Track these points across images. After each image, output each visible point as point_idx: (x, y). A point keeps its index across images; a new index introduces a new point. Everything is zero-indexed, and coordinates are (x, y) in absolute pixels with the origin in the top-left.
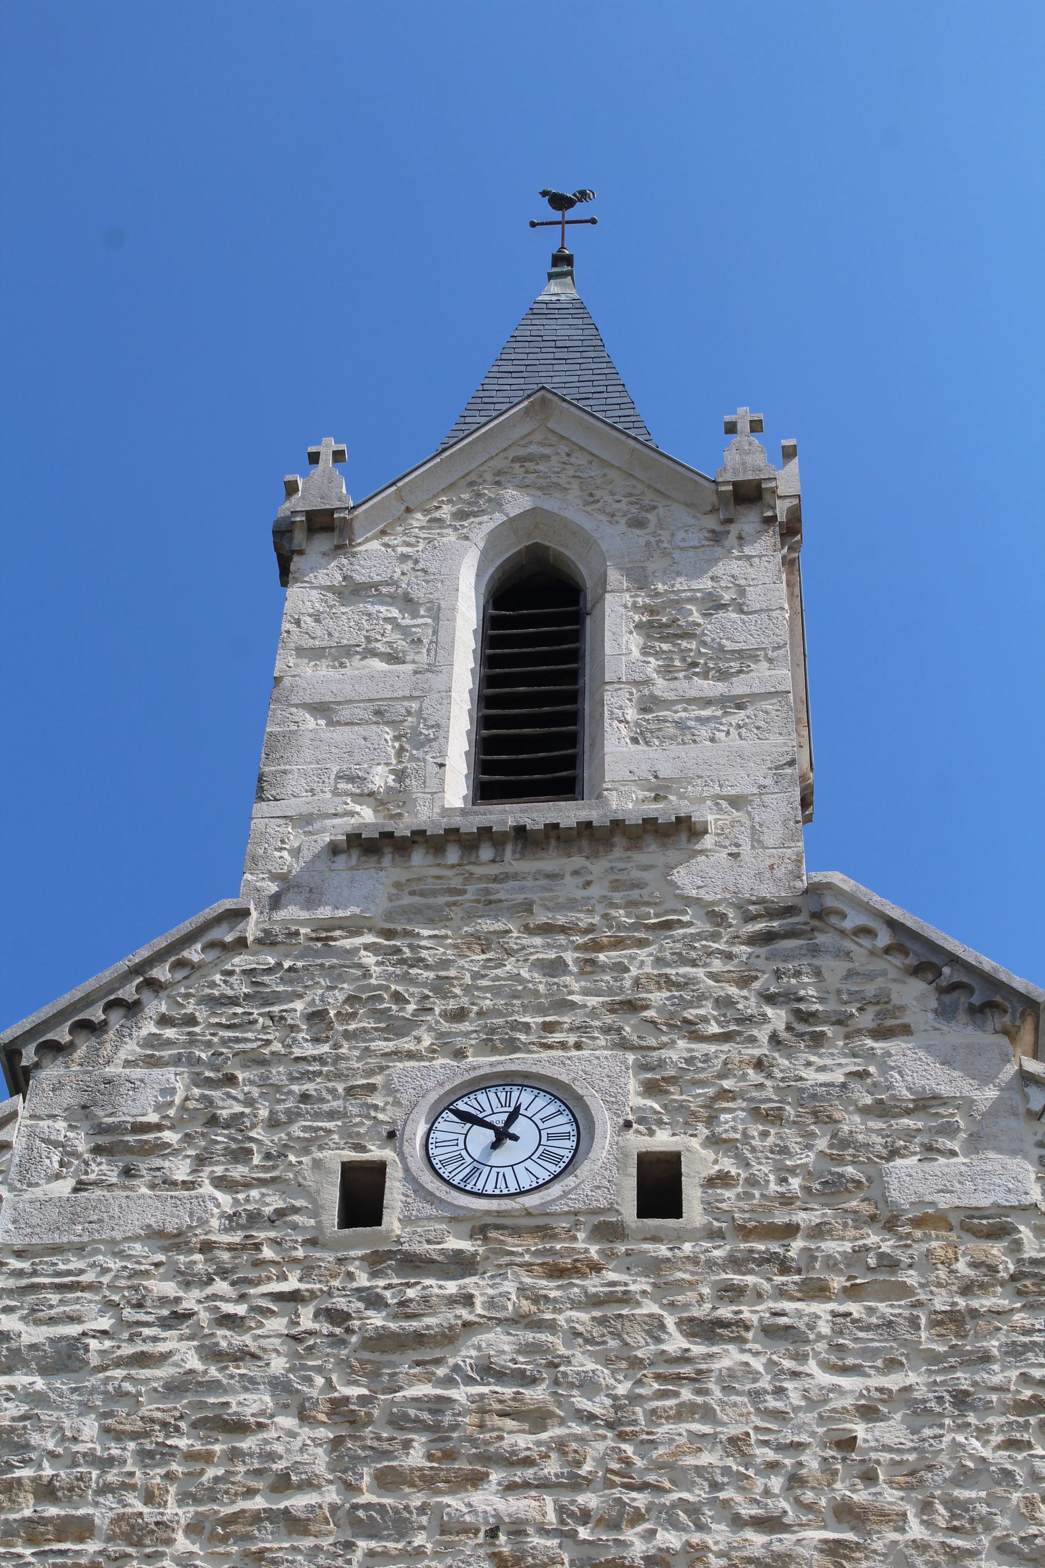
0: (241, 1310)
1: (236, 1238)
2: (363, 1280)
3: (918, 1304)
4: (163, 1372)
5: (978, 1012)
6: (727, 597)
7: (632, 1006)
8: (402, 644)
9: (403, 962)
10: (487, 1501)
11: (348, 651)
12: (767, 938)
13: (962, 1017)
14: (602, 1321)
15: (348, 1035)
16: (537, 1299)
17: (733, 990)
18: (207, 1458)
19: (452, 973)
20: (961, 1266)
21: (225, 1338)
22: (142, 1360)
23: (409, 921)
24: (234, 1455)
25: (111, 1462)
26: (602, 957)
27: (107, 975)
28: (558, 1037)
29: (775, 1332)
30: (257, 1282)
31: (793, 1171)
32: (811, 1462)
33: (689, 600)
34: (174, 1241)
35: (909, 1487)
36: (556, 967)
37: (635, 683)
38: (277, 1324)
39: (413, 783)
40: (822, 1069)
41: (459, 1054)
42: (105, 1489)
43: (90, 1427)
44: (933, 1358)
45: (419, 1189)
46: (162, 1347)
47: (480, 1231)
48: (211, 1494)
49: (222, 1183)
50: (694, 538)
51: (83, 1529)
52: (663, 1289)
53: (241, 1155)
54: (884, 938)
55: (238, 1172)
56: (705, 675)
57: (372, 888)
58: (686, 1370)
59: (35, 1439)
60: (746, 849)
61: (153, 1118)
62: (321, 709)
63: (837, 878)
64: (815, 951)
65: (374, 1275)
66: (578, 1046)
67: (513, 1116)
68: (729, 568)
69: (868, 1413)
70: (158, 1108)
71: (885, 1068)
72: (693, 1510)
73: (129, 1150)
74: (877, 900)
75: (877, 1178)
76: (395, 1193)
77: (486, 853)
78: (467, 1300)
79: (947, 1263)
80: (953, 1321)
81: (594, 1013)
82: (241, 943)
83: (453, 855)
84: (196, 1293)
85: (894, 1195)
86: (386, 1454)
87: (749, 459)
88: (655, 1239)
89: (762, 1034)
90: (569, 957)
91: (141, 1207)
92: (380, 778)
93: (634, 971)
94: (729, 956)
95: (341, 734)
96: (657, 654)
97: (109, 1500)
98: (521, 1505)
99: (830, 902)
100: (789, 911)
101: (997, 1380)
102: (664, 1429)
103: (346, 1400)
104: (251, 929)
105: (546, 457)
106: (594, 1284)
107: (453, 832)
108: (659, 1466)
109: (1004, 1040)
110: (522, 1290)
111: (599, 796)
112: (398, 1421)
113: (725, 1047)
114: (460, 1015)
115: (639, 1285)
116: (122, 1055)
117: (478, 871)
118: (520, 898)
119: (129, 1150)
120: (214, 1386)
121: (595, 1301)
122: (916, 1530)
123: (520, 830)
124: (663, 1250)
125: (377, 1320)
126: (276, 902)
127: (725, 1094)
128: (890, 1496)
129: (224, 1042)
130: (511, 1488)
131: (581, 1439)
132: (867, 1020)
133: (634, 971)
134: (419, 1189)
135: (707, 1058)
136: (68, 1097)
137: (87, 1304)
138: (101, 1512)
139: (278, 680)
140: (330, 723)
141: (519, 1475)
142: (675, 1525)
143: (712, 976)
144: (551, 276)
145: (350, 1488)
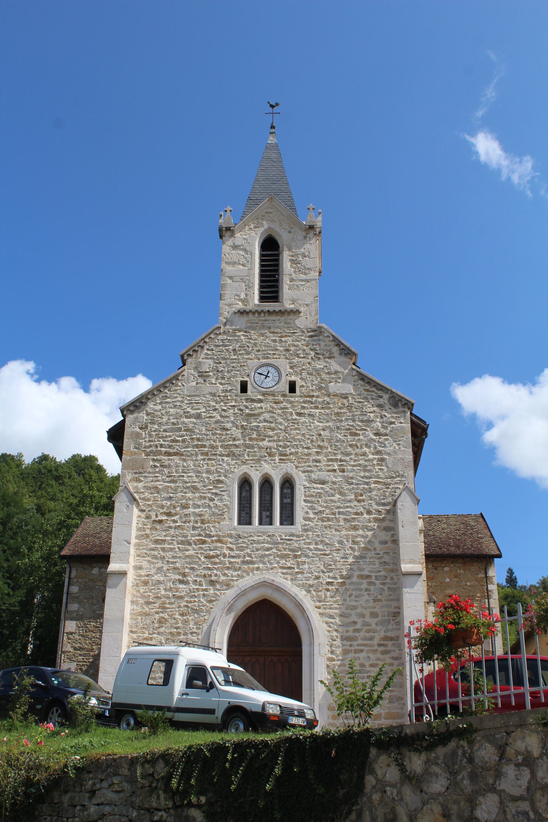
0: (225, 408)
1: (223, 394)
2: (245, 403)
3: (332, 411)
4: (214, 419)
5: (346, 355)
6: (307, 254)
7: (288, 350)
8: (245, 262)
9: (248, 338)
10: (265, 443)
11: (235, 263)
12: (311, 336)
13: (343, 355)
14: (283, 412)
15: (240, 354)
16: (273, 408)
17: (305, 348)
18: (222, 435)
19: (257, 342)
20: (339, 404)
21: (224, 413)
22: (211, 417)
23: (249, 329)
24: (227, 434)
25: (207, 435)
26: (283, 339)
27: (198, 340)
28: (275, 356)
29: (310, 415)
30: (228, 403)
31: (314, 385)
32: (314, 438)
33: (300, 254)
34: (214, 395)
35: (329, 443)
36: (275, 341)
37: (289, 275)
38: (231, 411)
39: (248, 297)
40: (320, 365)
41: (259, 359)
42: (207, 440)
43: (204, 429)
44: (335, 420)
45: (253, 386)
46: (214, 415)
47: (263, 395)
48: (224, 441)
49: (220, 384)
50: (301, 238)
51: (205, 446)
52: (293, 407)
53: (223, 378)
54: (331, 338)
55: (223, 381)
56: (302, 274)
57: (242, 321)
58: (296, 422)
59: (195, 431)
60: (308, 317)
61: (208, 370)
62: (231, 278)
63: (324, 325)
64: (319, 340)
65: (247, 402)
66: (279, 358)
67: (269, 372)
68: (307, 246)
69: (324, 430)
70: (209, 368)
71: (330, 365)
72: (297, 445)
73: (205, 376)
74: (331, 330)
75: (327, 386)
76: (249, 387)
77: (262, 315)
78: (262, 408)
79: (338, 403)
80: (338, 414)
81: (281, 352)
82: (220, 333)
83: (256, 315)
84: (218, 405)
85: (330, 390)
86: (250, 435)
87: (312, 219)
88: (291, 397)
89: (310, 357)
90: (277, 339)
91: (207, 388)
92: (243, 296)
93: (289, 343)
94: (305, 340)
95: (235, 284)
96: (293, 268)
97: (208, 441)
98: (271, 444)
99: (323, 330)
100: (315, 331)
101: (343, 425)
102: (293, 432)
103: (243, 425)
104: (222, 331)
105: (272, 213)
106: (282, 405)
107: (256, 311)
108: (292, 438)
109: (350, 360)
110: (270, 406)
111: (282, 302)
112: (252, 429)
113: (304, 359)
114: (259, 351)
115: (289, 406)
116: (201, 357)
117: (261, 318)
118: (269, 325)
119: (204, 376)
120: (222, 422)
121: (282, 409)
122: (330, 450)
123: (268, 311)
124: (293, 399)
125: (247, 411)
126: (225, 324)
127: (303, 369)
128: (326, 444)
129: (219, 355)
130: (269, 441)
131: (280, 433)
132: (327, 355)
133: (289, 343)
134: (253, 386)
135: (300, 362)
136: (193, 366)
137: (201, 406)
138: (207, 443)
139: (222, 270)
140: (233, 281)
141: (270, 439)
142: (294, 448)
143: (302, 344)
144: (271, 133)
145: (245, 440)
